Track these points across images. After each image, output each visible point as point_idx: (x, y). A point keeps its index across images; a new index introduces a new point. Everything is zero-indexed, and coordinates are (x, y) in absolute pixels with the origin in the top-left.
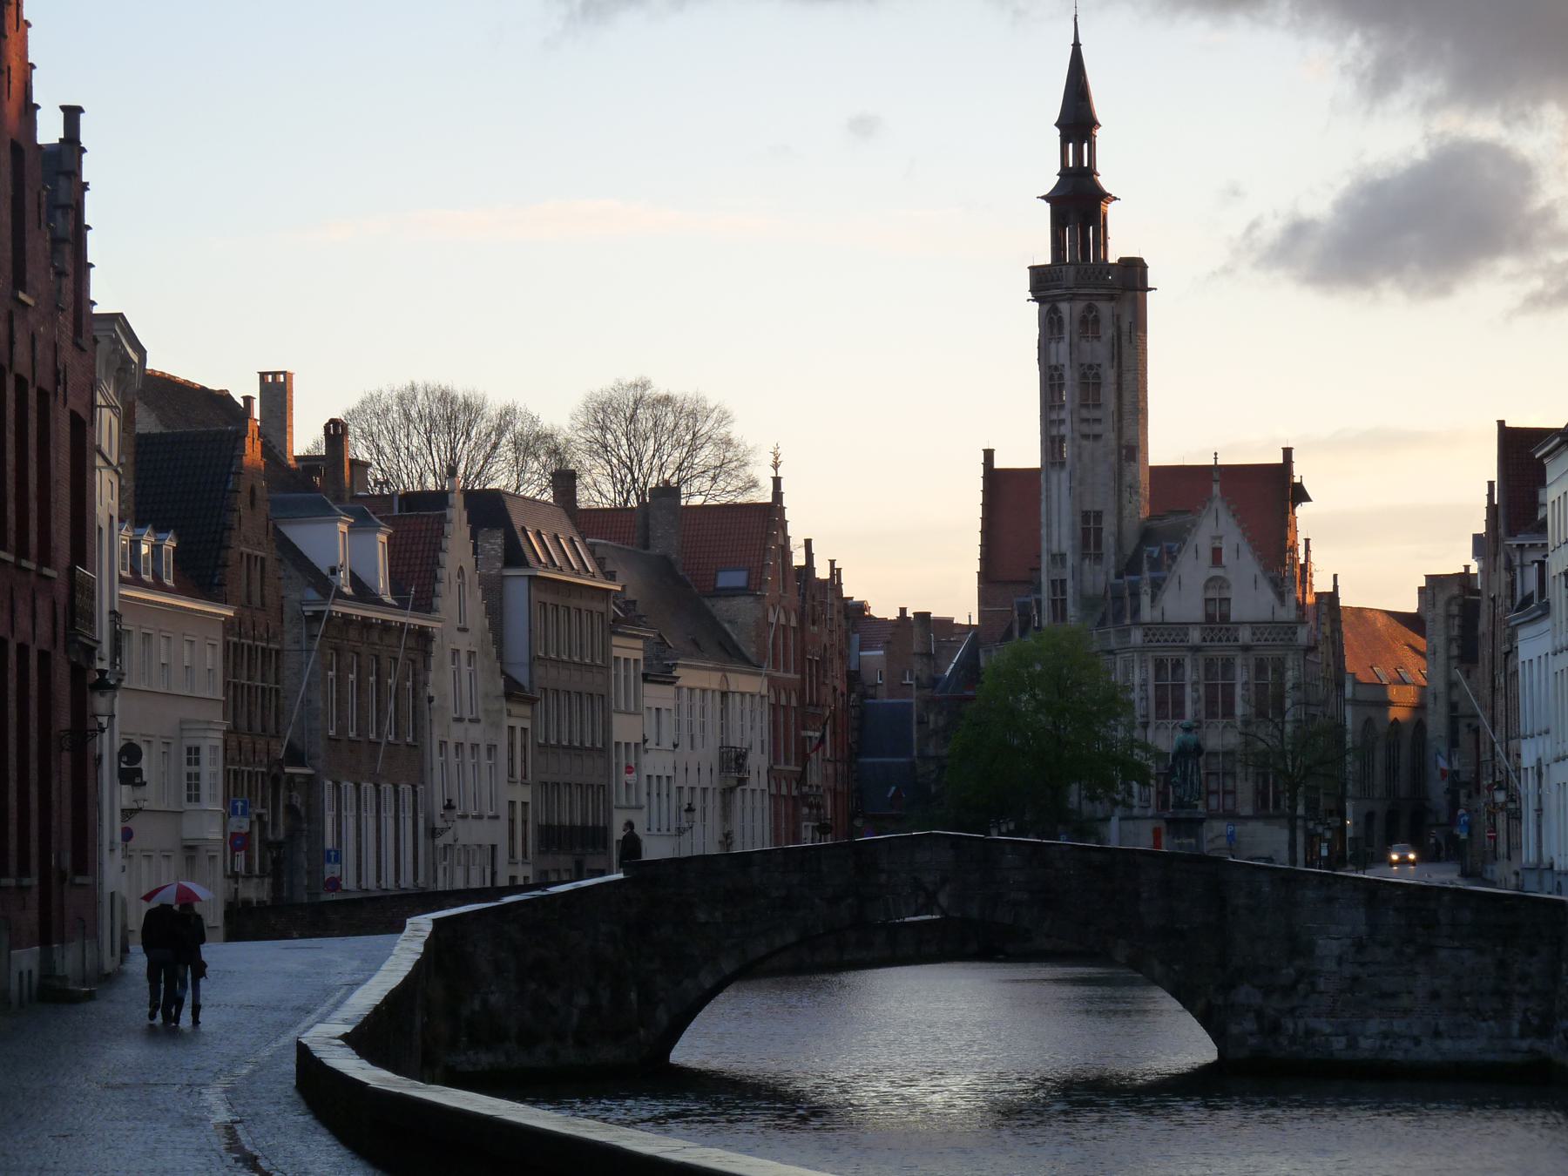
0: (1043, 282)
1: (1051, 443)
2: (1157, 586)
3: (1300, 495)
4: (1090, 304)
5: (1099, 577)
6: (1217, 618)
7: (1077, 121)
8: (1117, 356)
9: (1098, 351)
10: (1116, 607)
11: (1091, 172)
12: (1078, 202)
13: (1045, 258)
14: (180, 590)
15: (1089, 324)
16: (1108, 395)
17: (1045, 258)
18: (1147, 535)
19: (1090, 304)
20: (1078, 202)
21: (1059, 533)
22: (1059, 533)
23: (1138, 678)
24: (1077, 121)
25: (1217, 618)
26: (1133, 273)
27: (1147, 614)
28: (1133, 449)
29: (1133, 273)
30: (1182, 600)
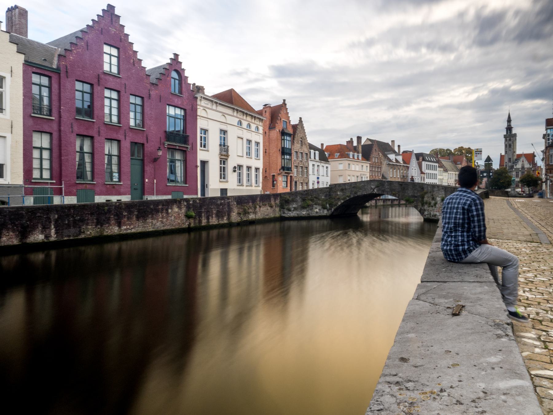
0: (505, 137)
1: (506, 152)
2: (516, 165)
3: (535, 156)
4: (510, 137)
5: (510, 164)
6: (523, 168)
7: (509, 120)
8: (513, 143)
9: (510, 142)
10: (512, 167)
11: (510, 125)
12: (509, 129)
13: (505, 133)
14: (362, 160)
15: (510, 140)
16: (512, 147)
17: (505, 133)
18: (516, 160)
19: (510, 137)
20: (509, 129)
21: (506, 160)
22: (506, 160)
23: (514, 173)
24: (509, 120)
25: (523, 168)
26: (515, 135)
27: (515, 167)
28: (515, 152)
29: (515, 135)
30: (519, 166)
